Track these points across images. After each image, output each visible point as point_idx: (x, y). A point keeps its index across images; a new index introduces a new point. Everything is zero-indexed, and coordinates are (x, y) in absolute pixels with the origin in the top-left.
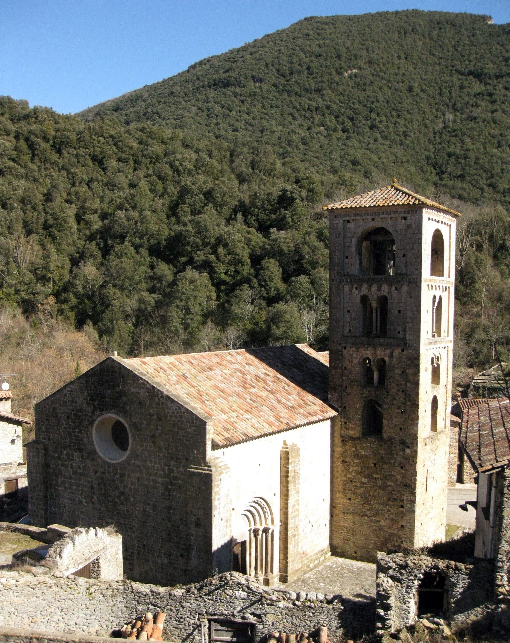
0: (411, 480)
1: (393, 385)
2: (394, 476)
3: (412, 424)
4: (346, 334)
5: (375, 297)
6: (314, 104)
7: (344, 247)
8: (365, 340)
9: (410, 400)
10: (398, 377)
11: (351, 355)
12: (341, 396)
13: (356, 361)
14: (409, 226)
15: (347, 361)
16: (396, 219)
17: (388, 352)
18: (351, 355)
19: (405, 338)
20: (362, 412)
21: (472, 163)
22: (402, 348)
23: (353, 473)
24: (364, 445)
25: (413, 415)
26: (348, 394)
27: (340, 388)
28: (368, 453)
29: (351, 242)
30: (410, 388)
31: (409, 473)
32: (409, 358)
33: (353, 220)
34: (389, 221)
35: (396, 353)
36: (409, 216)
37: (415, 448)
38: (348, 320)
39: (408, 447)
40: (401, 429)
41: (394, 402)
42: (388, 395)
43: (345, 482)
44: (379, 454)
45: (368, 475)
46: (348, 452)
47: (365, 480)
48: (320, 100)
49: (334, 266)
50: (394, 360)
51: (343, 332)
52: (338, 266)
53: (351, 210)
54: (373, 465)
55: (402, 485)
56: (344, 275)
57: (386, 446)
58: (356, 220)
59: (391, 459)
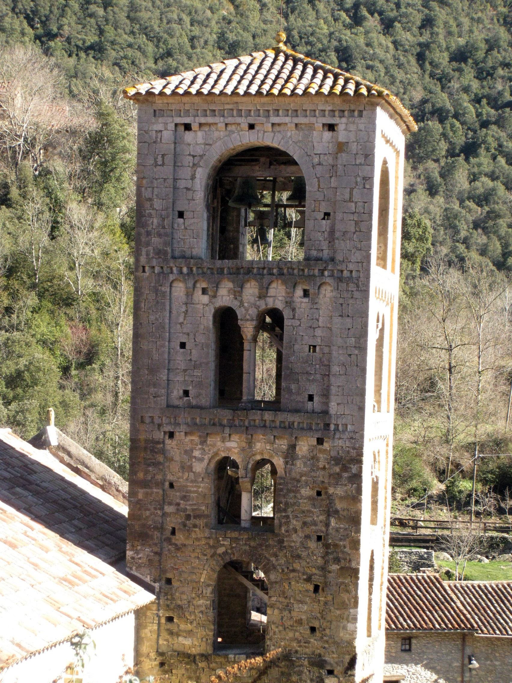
1: (295, 523)
3: (341, 617)
4: (176, 402)
5: (253, 312)
7: (175, 188)
8: (225, 415)
9: (337, 560)
11: (189, 453)
13: (199, 467)
14: (341, 147)
15: (175, 467)
16: (311, 127)
17: (283, 444)
18: (186, 452)
19: (326, 413)
21: (122, 16)
22: (319, 435)
25: (345, 596)
26: (178, 548)
27: (157, 534)
29: (193, 178)
30: (337, 530)
32: (337, 460)
33: (201, 125)
34: (291, 132)
35: (304, 447)
38: (182, 366)
40: (313, 629)
41: (297, 566)
49: (148, 234)
50: (298, 463)
51: (168, 395)
52: (159, 235)
53: (197, 100)
56: (173, 257)
58: (209, 125)
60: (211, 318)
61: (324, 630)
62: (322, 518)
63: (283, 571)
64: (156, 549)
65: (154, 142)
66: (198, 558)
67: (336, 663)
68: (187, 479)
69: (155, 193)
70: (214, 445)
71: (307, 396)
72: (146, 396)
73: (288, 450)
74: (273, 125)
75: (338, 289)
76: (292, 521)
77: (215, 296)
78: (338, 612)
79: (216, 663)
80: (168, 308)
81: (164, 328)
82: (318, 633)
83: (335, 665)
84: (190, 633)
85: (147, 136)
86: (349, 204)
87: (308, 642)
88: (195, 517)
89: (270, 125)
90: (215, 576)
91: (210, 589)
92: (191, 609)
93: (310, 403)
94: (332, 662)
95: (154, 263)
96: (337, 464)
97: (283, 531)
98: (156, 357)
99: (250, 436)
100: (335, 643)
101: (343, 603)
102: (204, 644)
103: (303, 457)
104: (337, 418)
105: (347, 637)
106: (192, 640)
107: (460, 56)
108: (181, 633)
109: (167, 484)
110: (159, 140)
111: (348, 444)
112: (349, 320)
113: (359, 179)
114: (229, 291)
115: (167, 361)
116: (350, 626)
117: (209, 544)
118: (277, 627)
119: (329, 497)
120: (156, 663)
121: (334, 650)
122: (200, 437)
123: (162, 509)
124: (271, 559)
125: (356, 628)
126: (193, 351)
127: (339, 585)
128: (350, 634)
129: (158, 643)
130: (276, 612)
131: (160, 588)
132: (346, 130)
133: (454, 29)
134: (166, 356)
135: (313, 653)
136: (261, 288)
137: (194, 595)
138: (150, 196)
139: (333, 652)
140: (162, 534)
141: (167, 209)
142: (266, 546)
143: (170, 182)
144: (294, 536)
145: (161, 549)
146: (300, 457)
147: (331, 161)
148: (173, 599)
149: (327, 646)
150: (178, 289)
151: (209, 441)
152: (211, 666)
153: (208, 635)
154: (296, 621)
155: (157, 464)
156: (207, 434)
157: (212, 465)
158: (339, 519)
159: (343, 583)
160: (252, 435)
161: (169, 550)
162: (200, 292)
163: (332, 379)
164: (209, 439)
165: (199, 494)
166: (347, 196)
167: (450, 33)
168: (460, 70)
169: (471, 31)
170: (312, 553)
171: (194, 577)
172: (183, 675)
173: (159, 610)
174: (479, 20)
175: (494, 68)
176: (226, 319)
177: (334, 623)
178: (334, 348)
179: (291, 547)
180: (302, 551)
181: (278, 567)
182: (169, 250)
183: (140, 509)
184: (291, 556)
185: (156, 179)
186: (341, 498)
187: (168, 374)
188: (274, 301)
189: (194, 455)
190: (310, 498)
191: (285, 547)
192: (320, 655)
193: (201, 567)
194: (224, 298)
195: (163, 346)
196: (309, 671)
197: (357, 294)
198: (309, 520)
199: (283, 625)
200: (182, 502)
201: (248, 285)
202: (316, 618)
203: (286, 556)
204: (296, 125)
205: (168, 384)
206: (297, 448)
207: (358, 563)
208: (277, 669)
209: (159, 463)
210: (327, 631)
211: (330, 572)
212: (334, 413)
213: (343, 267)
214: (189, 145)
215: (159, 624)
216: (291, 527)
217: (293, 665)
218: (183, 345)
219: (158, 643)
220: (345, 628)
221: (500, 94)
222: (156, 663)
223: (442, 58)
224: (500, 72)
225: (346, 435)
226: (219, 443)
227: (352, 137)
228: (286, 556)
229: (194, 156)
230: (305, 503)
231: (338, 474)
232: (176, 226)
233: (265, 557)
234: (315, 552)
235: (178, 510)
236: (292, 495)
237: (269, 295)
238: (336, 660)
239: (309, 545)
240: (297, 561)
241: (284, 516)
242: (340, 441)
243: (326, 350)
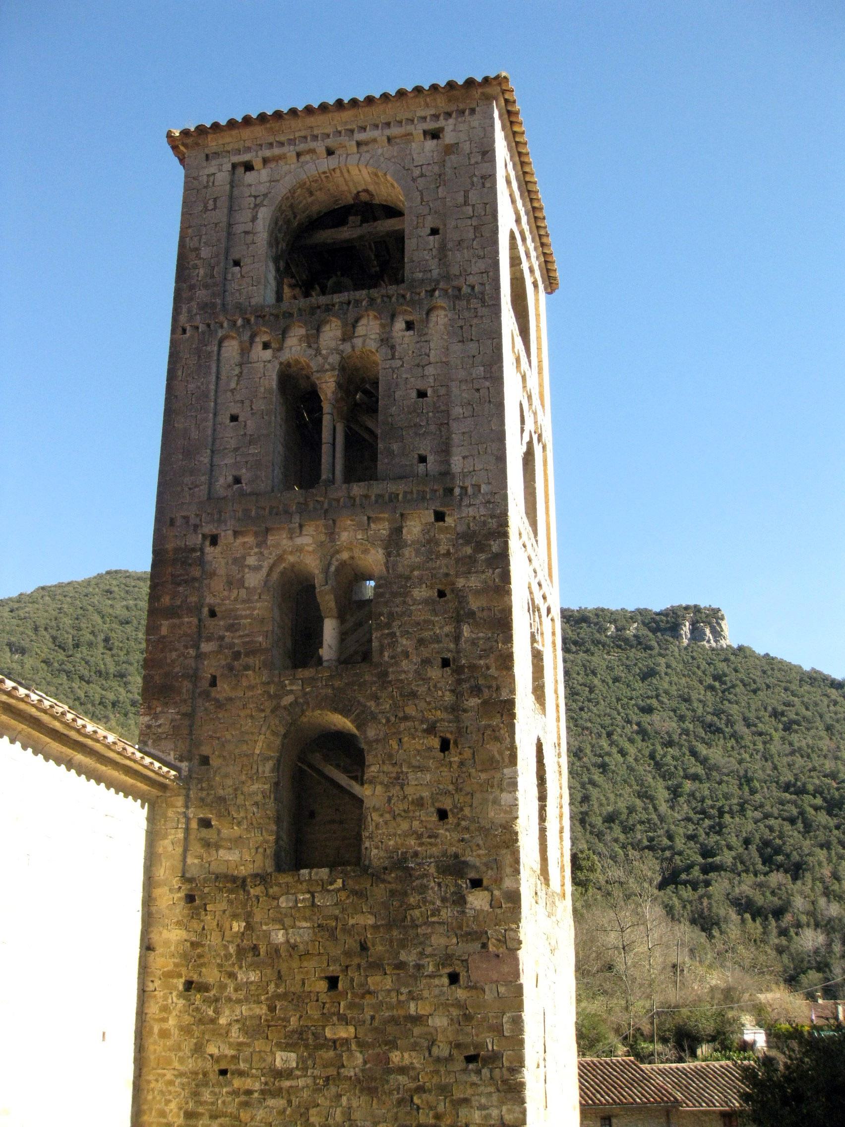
0: (498, 1030)
1: (405, 642)
2: (417, 1020)
3: (489, 783)
4: (222, 492)
5: (334, 359)
6: (111, 696)
9: (476, 690)
10: (420, 614)
11: (239, 562)
12: (190, 715)
13: (253, 580)
14: (450, 149)
15: (217, 585)
17: (382, 529)
18: (235, 561)
19: (446, 474)
20: (277, 768)
23: (235, 1031)
24: (283, 902)
25: (493, 748)
26: (219, 705)
27: (187, 685)
28: (303, 932)
29: (254, 219)
30: (474, 643)
31: (489, 996)
32: (467, 537)
33: (265, 161)
34: (382, 149)
36: (448, 125)
37: (508, 883)
38: (233, 443)
39: (477, 884)
40: (443, 815)
41: (410, 710)
42: (383, 687)
43: (198, 1082)
44: (347, 930)
45: (300, 1033)
46: (214, 939)
47: (283, 1059)
48: (121, 690)
50: (407, 552)
51: (211, 485)
52: (206, 286)
54: (323, 985)
55: (459, 1057)
57: (379, 892)
59: (403, 944)
61: (462, 809)
63: (388, 721)
64: (185, 709)
65: (206, 187)
66: (252, 717)
67: (486, 865)
68: (236, 599)
69: (203, 240)
70: (277, 545)
71: (416, 456)
72: (179, 489)
73: (390, 536)
74: (359, 144)
75: (454, 309)
76: (400, 640)
77: (280, 349)
78: (483, 776)
79: (279, 885)
80: (214, 370)
81: (207, 397)
82: (451, 819)
83: (484, 869)
84: (237, 842)
85: (195, 182)
86: (464, 208)
87: (436, 836)
88: (247, 655)
89: (354, 143)
90: (278, 742)
91: (269, 765)
92: (240, 800)
94: (478, 864)
96: (468, 543)
97: (386, 658)
98: (194, 434)
99: (331, 522)
100: (481, 829)
101: (492, 759)
102: (259, 857)
103: (413, 542)
104: (464, 476)
105: (501, 818)
106: (241, 852)
107: (610, 819)
108: (223, 843)
109: (205, 610)
110: (211, 184)
111: (483, 511)
112: (473, 346)
113: (475, 179)
114: (300, 340)
115: (210, 439)
116: (505, 797)
117: (268, 693)
118: (381, 815)
120: (179, 895)
121: (481, 843)
122: (256, 534)
123: (198, 648)
124: (368, 704)
125: (516, 799)
126: (249, 423)
127: (482, 730)
128: (506, 812)
129: (184, 860)
130: (379, 789)
131: (190, 770)
132: (454, 130)
133: (604, 801)
134: (210, 432)
135: (445, 854)
136: (345, 324)
137: (244, 778)
138: (197, 245)
139: (478, 845)
140: (195, 686)
141: (217, 256)
142: (360, 685)
143: (224, 225)
144: (404, 663)
145: (194, 710)
146: (409, 542)
147: (436, 169)
148: (211, 787)
149: (467, 836)
151: (271, 539)
152: (271, 891)
153: (267, 842)
154: (413, 802)
155: (189, 582)
156: (267, 530)
157: (275, 576)
158: (476, 625)
159: (489, 726)
160: (334, 521)
161: (206, 709)
162: (260, 347)
163: (454, 425)
164: (270, 538)
165: (255, 619)
166: (461, 200)
167: (601, 805)
168: (611, 828)
169: (616, 803)
170: (435, 686)
171: (245, 748)
172: (224, 911)
173: (187, 807)
174: (621, 795)
175: (634, 825)
177: (478, 795)
178: (453, 384)
179: (402, 681)
180: (418, 685)
181: (380, 716)
182: (218, 301)
183: (162, 651)
184: (401, 695)
185: (205, 226)
186: (477, 593)
187: (212, 457)
188: (364, 341)
189: (247, 563)
190: (426, 602)
191: (390, 682)
192: (456, 856)
193: (256, 731)
194: (293, 349)
195: (205, 420)
196: (439, 884)
197: (483, 311)
198: (426, 634)
199: (391, 811)
200: (227, 634)
201: (327, 328)
202: (447, 793)
203: (392, 697)
204: (389, 139)
205: (212, 471)
206: (405, 531)
207: (513, 691)
208: (382, 886)
209: (195, 579)
210: (467, 811)
211: (465, 711)
212: (459, 470)
213: (460, 282)
214: (250, 185)
215: (187, 830)
216: (399, 650)
217: (411, 875)
218: (234, 418)
219: (184, 860)
220: (496, 802)
221: (640, 841)
222: (179, 895)
223: (598, 821)
224: (638, 827)
225: (480, 499)
226: (285, 542)
227: (463, 137)
228: (392, 697)
229: (256, 197)
230: (419, 610)
231: (470, 557)
232: (229, 277)
233: (359, 701)
234: (439, 685)
235: (220, 646)
236: (398, 600)
237: (356, 335)
238: (484, 860)
239: (429, 675)
240: (410, 702)
241: (388, 634)
242: (470, 509)
243: (442, 391)
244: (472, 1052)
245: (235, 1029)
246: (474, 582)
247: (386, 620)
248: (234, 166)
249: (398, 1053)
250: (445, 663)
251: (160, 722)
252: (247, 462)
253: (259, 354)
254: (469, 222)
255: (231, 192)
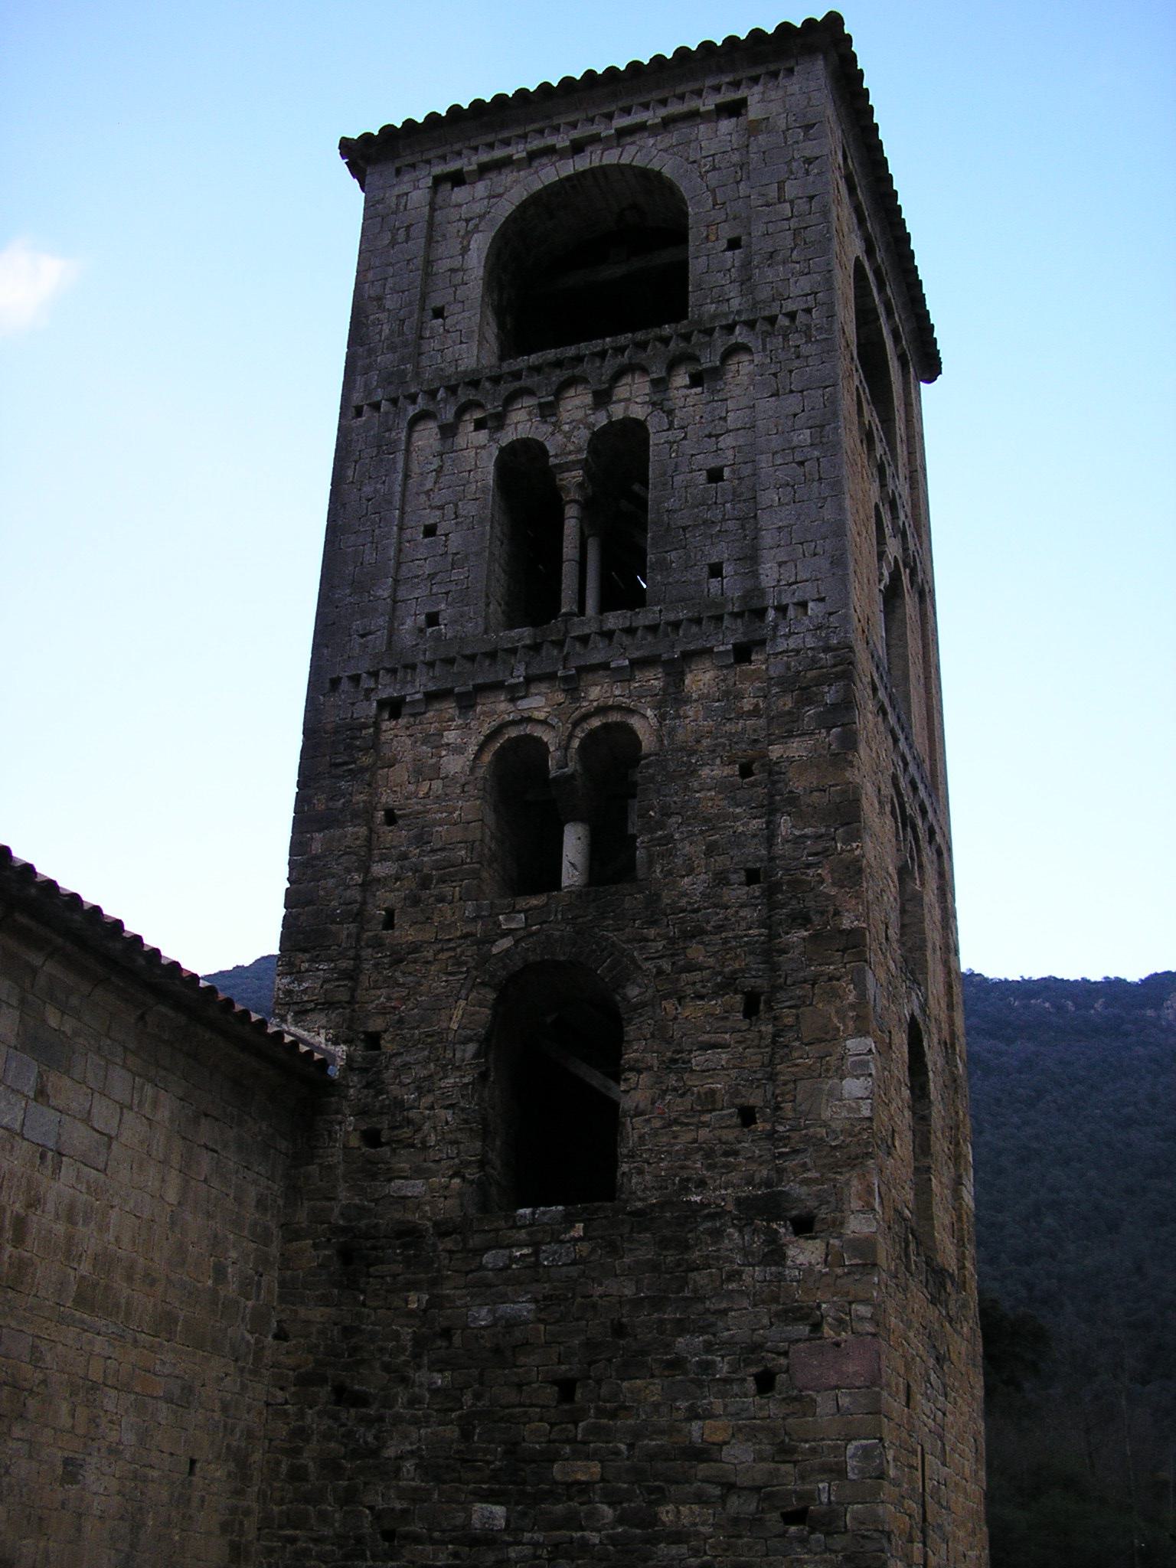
2: (701, 1453)
5: (583, 436)
9: (802, 919)
10: (709, 801)
11: (434, 739)
12: (351, 976)
13: (454, 764)
15: (400, 774)
29: (465, 250)
32: (787, 683)
36: (754, 96)
39: (804, 1226)
40: (747, 1116)
50: (690, 710)
52: (392, 348)
59: (682, 1327)
60: (492, 468)
62: (756, 824)
64: (344, 964)
65: (395, 213)
68: (427, 796)
71: (706, 569)
80: (400, 465)
93: (714, 583)
95: (379, 395)
98: (370, 557)
112: (792, 403)
119: (773, 770)
123: (367, 870)
128: (850, 1109)
132: (762, 101)
141: (410, 304)
143: (419, 262)
146: (695, 696)
147: (736, 158)
150: (426, 432)
163: (764, 519)
166: (773, 193)
176: (523, 474)
190: (723, 787)
194: (520, 427)
205: (394, 609)
214: (460, 206)
218: (430, 531)
220: (835, 1095)
229: (467, 221)
231: (790, 713)
241: (661, 838)
243: (747, 470)
244: (794, 1504)
245: (409, 1465)
246: (797, 748)
247: (658, 817)
248: (438, 180)
249: (671, 1507)
250: (752, 877)
251: (305, 985)
252: (447, 593)
253: (470, 437)
254: (785, 225)
255: (431, 217)
